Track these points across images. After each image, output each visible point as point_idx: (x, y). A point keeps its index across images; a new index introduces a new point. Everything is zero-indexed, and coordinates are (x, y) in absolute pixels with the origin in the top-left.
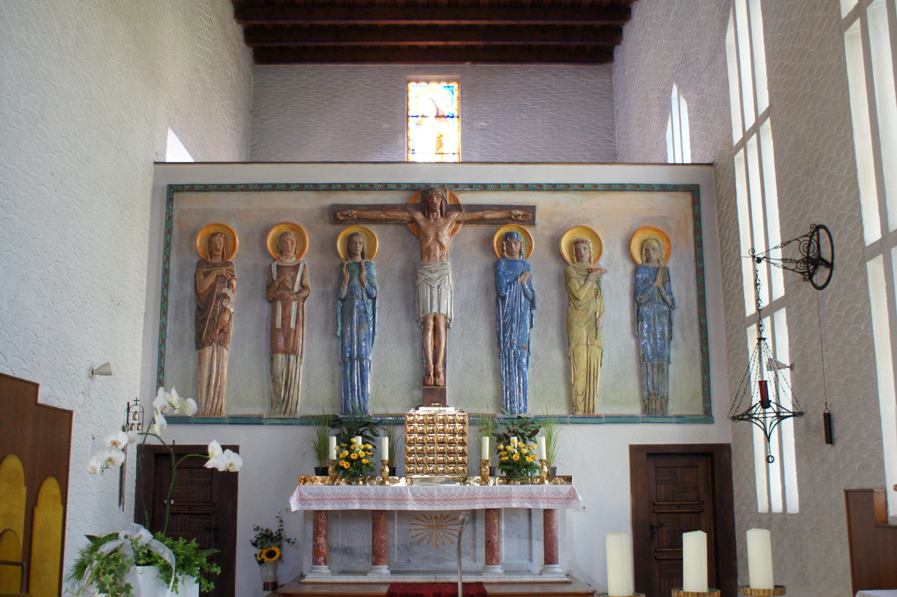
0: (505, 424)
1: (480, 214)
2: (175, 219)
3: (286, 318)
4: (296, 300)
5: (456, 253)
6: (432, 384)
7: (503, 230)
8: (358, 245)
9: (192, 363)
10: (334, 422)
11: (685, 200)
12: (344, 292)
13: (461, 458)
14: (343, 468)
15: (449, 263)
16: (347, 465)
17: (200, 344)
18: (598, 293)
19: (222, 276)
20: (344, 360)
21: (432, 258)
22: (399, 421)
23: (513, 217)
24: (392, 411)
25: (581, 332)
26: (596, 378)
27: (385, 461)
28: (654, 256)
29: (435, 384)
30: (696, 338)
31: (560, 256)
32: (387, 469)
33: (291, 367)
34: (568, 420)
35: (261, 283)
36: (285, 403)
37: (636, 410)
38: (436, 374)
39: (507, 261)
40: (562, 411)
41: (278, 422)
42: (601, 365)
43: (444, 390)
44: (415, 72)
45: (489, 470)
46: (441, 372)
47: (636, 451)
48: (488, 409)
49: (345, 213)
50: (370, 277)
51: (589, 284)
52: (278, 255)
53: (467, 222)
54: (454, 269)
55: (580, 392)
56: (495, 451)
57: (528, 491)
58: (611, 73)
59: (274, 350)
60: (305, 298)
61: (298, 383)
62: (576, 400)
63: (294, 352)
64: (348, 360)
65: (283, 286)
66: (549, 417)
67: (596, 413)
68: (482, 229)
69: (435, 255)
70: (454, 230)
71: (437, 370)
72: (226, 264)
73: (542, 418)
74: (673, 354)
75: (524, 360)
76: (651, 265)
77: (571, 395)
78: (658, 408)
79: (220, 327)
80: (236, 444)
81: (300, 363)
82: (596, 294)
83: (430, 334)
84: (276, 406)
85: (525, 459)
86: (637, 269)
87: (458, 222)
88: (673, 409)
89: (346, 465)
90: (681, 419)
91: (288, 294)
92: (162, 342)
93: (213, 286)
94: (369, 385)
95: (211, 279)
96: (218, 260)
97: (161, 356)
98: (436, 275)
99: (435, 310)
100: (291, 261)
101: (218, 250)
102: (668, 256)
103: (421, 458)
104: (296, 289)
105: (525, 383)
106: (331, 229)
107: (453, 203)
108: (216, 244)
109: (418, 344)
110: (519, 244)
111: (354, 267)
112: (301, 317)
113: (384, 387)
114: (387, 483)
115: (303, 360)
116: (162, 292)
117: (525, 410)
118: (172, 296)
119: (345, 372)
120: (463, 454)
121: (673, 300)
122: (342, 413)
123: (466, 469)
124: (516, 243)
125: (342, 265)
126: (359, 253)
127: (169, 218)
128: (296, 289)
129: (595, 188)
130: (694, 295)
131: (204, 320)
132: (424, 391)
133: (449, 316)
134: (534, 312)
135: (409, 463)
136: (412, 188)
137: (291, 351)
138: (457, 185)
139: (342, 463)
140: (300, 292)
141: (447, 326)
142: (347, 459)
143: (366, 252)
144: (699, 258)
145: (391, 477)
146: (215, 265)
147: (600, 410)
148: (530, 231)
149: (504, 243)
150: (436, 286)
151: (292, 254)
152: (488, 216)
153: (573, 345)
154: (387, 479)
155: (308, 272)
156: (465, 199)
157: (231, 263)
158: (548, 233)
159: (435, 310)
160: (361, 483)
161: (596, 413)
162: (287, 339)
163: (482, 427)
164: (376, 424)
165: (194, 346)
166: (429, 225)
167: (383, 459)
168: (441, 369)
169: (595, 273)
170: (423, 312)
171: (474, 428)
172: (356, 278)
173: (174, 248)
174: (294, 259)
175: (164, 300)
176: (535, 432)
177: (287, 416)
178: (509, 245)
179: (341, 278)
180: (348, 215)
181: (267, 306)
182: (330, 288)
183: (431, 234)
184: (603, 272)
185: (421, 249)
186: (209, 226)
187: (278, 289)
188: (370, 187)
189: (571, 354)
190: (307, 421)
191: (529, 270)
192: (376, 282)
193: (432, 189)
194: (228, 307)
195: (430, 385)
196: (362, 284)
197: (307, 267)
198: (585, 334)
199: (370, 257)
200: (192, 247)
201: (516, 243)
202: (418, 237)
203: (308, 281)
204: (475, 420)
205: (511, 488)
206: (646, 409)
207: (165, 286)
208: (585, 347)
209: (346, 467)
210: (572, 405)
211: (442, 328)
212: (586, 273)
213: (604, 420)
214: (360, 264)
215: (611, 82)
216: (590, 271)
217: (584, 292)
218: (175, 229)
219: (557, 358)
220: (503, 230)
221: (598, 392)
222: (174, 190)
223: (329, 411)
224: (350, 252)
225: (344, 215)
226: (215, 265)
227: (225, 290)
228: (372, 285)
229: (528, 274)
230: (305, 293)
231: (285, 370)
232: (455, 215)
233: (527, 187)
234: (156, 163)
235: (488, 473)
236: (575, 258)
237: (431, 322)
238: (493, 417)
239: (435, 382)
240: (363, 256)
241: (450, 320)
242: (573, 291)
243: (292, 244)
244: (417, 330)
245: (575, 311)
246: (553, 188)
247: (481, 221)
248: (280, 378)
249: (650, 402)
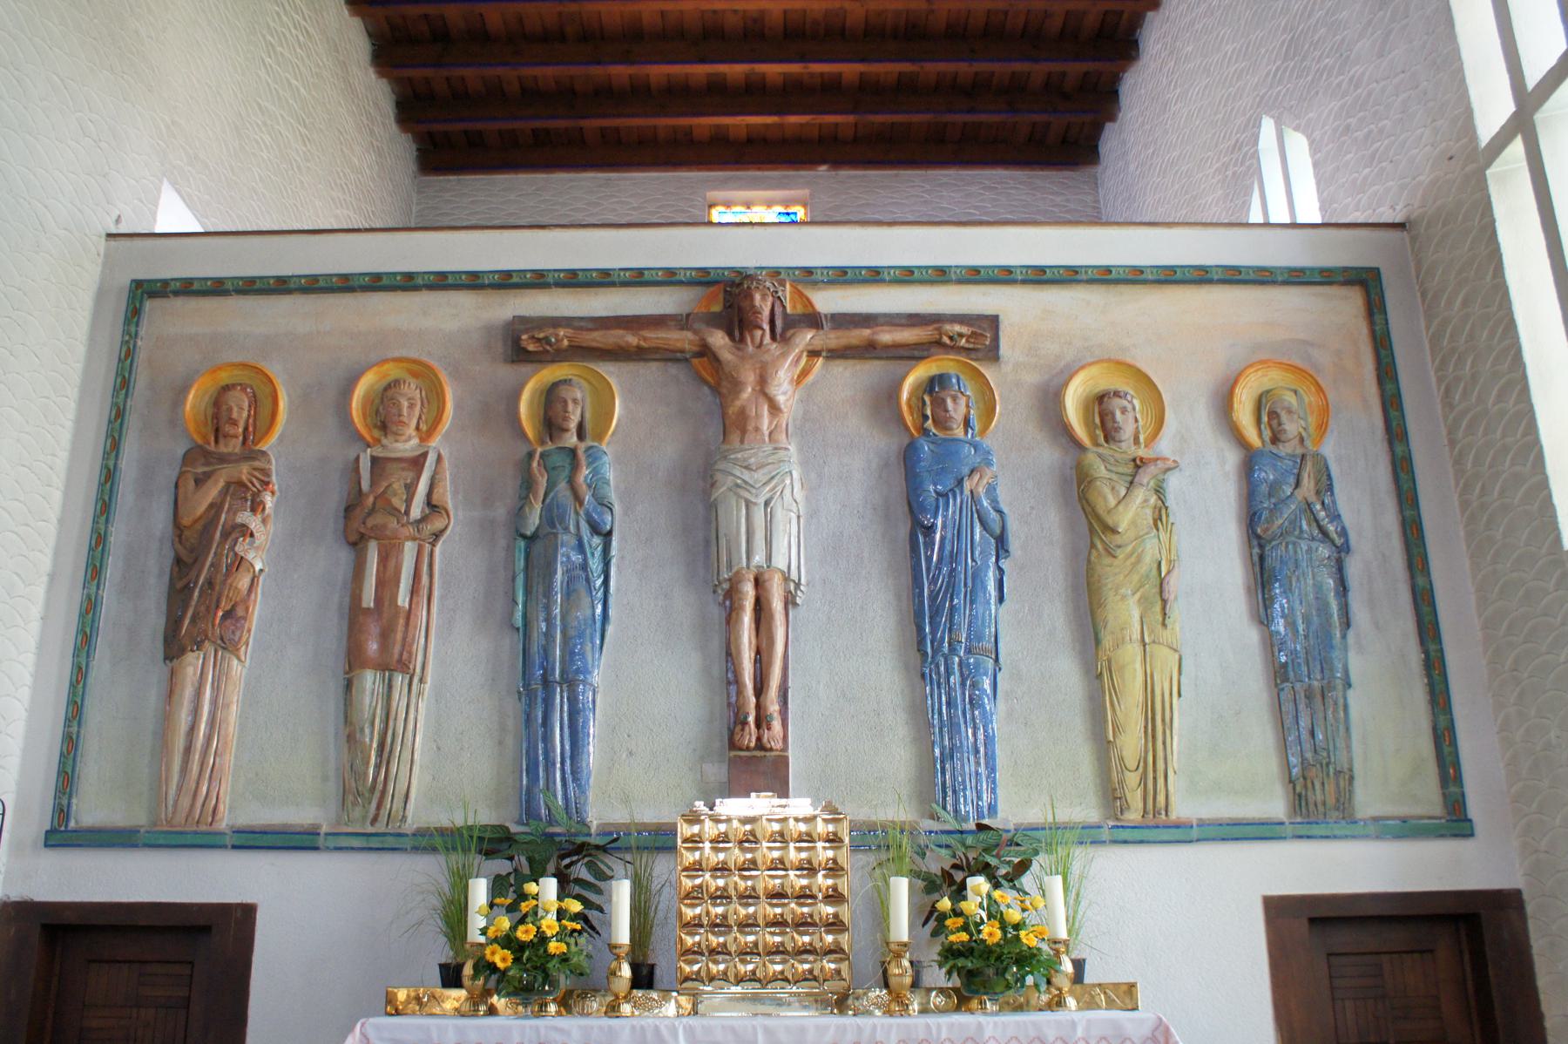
0: (947, 846)
1: (867, 332)
2: (141, 356)
3: (387, 583)
4: (414, 539)
6: (753, 744)
7: (918, 374)
8: (571, 407)
9: (153, 698)
10: (494, 843)
11: (1347, 306)
12: (533, 520)
13: (829, 938)
14: (493, 968)
15: (792, 448)
16: (504, 960)
17: (174, 647)
18: (1160, 516)
19: (241, 484)
20: (526, 685)
21: (749, 436)
22: (661, 840)
23: (946, 340)
24: (648, 816)
26: (1168, 724)
27: (620, 947)
28: (1291, 428)
29: (760, 746)
30: (1405, 624)
31: (1065, 430)
32: (626, 971)
33: (394, 704)
34: (1105, 834)
35: (335, 499)
36: (377, 794)
37: (1275, 806)
38: (762, 721)
39: (934, 441)
40: (1087, 811)
41: (356, 842)
42: (1179, 695)
43: (784, 761)
44: (722, 186)
45: (910, 971)
46: (776, 715)
47: (1279, 910)
48: (896, 809)
49: (541, 335)
50: (597, 484)
51: (1140, 495)
52: (376, 433)
53: (836, 354)
54: (805, 463)
55: (1131, 762)
56: (930, 918)
57: (1032, 1034)
58: (1095, 184)
59: (354, 659)
60: (437, 535)
61: (410, 744)
62: (1121, 782)
63: (404, 666)
64: (537, 686)
65: (383, 503)
66: (1057, 827)
67: (1173, 816)
68: (866, 373)
69: (757, 429)
70: (804, 373)
71: (765, 710)
72: (251, 454)
73: (1044, 829)
74: (1356, 664)
75: (986, 684)
76: (1284, 449)
77: (1109, 769)
78: (1331, 801)
79: (225, 605)
80: (249, 901)
81: (419, 694)
82: (1157, 520)
83: (747, 618)
84: (355, 804)
85: (1017, 938)
86: (1250, 462)
87: (814, 354)
88: (1368, 801)
89: (501, 958)
91: (393, 523)
92: (85, 640)
93: (216, 507)
94: (591, 749)
95: (212, 491)
96: (234, 446)
97: (80, 675)
98: (760, 476)
99: (759, 558)
100: (407, 445)
101: (234, 423)
102: (1322, 427)
103: (721, 940)
104: (416, 511)
105: (989, 740)
106: (506, 373)
107: (800, 310)
108: (230, 409)
109: (716, 644)
110: (963, 401)
111: (560, 460)
112: (425, 579)
113: (631, 753)
114: (626, 1008)
115: (427, 686)
116: (95, 522)
117: (992, 809)
118: (118, 535)
119: (529, 719)
120: (835, 925)
121: (1343, 533)
122: (520, 823)
123: (844, 966)
124: (955, 399)
125: (530, 455)
126: (573, 425)
127: (128, 354)
128: (416, 511)
129: (1136, 277)
130: (1391, 519)
131: (187, 590)
132: (733, 762)
133: (794, 575)
134: (1004, 564)
135: (690, 953)
136: (703, 279)
137: (396, 663)
138: (809, 271)
139: (493, 953)
140: (424, 519)
141: (790, 601)
142: (508, 941)
143: (588, 426)
144: (1395, 433)
145: (638, 993)
146: (223, 459)
147: (1183, 808)
148: (988, 372)
149: (927, 399)
150: (761, 501)
151: (411, 431)
152: (886, 337)
153: (1107, 641)
154: (627, 998)
156: (828, 301)
157: (264, 453)
158: (1031, 378)
160: (552, 1008)
161: (1173, 816)
162: (385, 636)
163: (884, 856)
164: (603, 849)
165: (161, 655)
166: (743, 358)
167: (613, 942)
168: (773, 708)
169: (1152, 469)
170: (730, 567)
171: (862, 858)
172: (562, 486)
173: (133, 421)
174: (415, 441)
175: (99, 541)
176: (1023, 867)
177: (380, 827)
178: (939, 403)
179: (527, 485)
180: (547, 340)
181: (345, 556)
182: (501, 512)
183: (749, 378)
185: (724, 415)
186: (215, 370)
187: (372, 511)
188: (604, 279)
189: (1102, 665)
190: (429, 841)
191: (989, 464)
192: (613, 497)
193: (748, 277)
194: (250, 556)
195: (748, 749)
196: (578, 499)
197: (446, 463)
198: (1136, 614)
199: (599, 437)
200: (174, 421)
201: (955, 399)
202: (716, 390)
203: (447, 495)
204: (870, 838)
205: (980, 1026)
206: (1299, 801)
207: (104, 507)
208: (1138, 649)
209: (501, 965)
210: (1112, 797)
211: (777, 605)
212: (1129, 469)
213: (1195, 833)
214: (573, 452)
215: (1097, 201)
216: (1138, 464)
217: (1130, 514)
218: (141, 380)
219: (1066, 672)
220: (918, 374)
221: (1175, 762)
222: (145, 291)
223: (485, 816)
224: (551, 425)
225: (539, 340)
226: (223, 459)
227: (245, 517)
229: (989, 473)
230: (438, 524)
231: (379, 711)
232: (806, 337)
233: (975, 276)
234: (110, 236)
235: (908, 980)
236: (1099, 433)
237: (749, 590)
238: (911, 831)
239: (759, 739)
240: (581, 434)
241: (798, 585)
242: (1101, 511)
243: (411, 406)
244: (716, 613)
245: (1107, 560)
246: (1039, 276)
247: (868, 350)
248: (367, 731)
249: (1309, 785)
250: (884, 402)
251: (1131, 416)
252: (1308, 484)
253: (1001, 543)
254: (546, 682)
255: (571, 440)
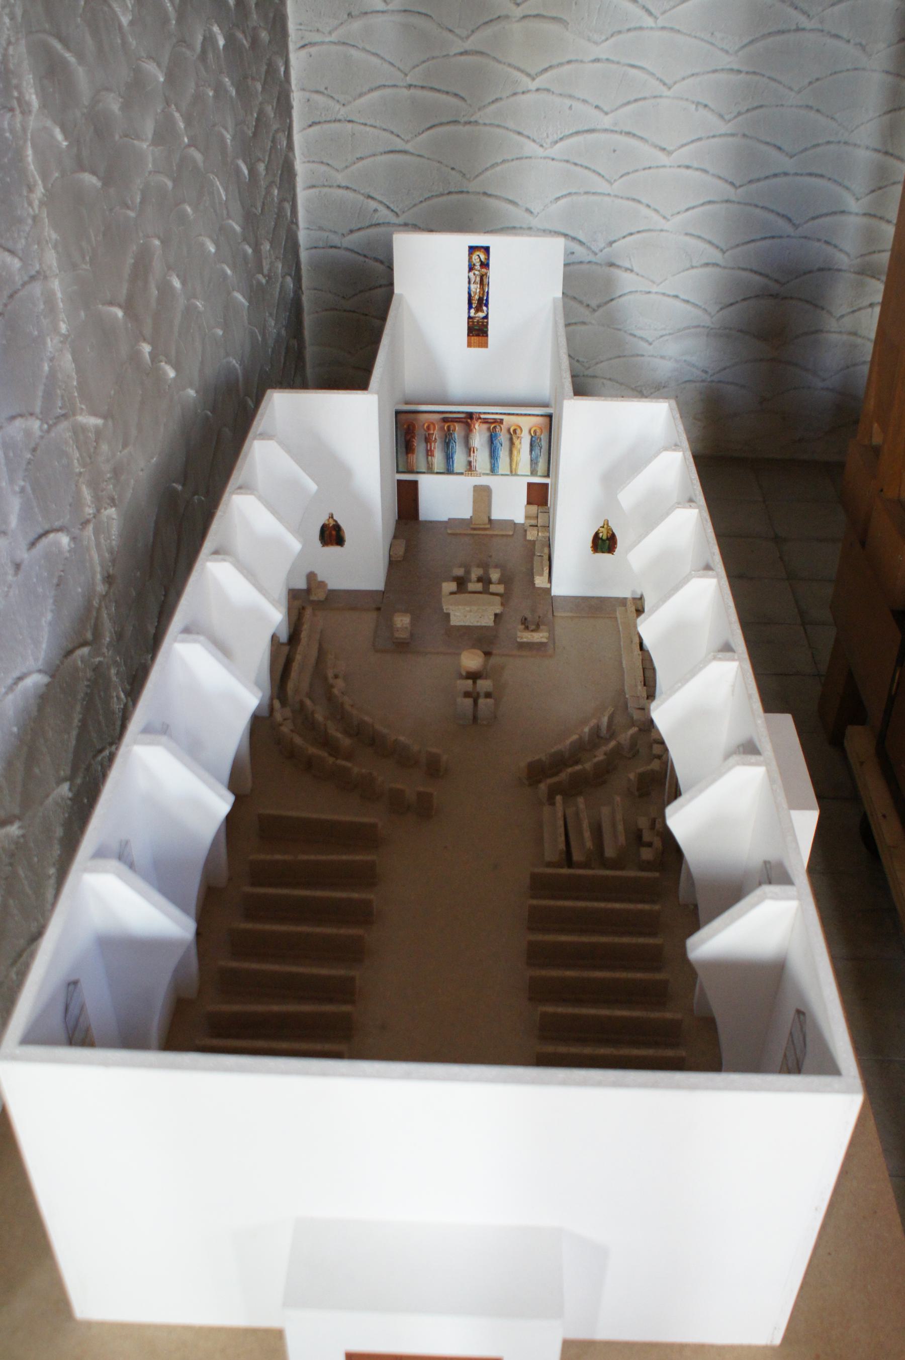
5: (480, 431)
7: (493, 426)
12: (447, 440)
17: (407, 453)
18: (520, 443)
25: (515, 452)
28: (538, 434)
30: (547, 457)
37: (529, 474)
59: (428, 455)
86: (532, 437)
88: (539, 473)
90: (541, 476)
99: (473, 446)
100: (432, 432)
106: (442, 424)
128: (434, 439)
134: (502, 448)
136: (466, 413)
137: (432, 455)
141: (477, 450)
147: (519, 473)
155: (437, 436)
156: (482, 416)
159: (473, 446)
179: (446, 437)
182: (443, 440)
183: (473, 425)
184: (522, 438)
188: (455, 412)
199: (455, 431)
203: (437, 438)
210: (511, 472)
216: (518, 437)
217: (517, 442)
219: (508, 459)
220: (493, 426)
228: (455, 439)
232: (480, 420)
237: (472, 449)
240: (453, 431)
244: (468, 451)
246: (509, 414)
250: (489, 429)
251: (518, 431)
252: (538, 441)
253: (502, 445)
254: (450, 458)
255: (451, 432)
